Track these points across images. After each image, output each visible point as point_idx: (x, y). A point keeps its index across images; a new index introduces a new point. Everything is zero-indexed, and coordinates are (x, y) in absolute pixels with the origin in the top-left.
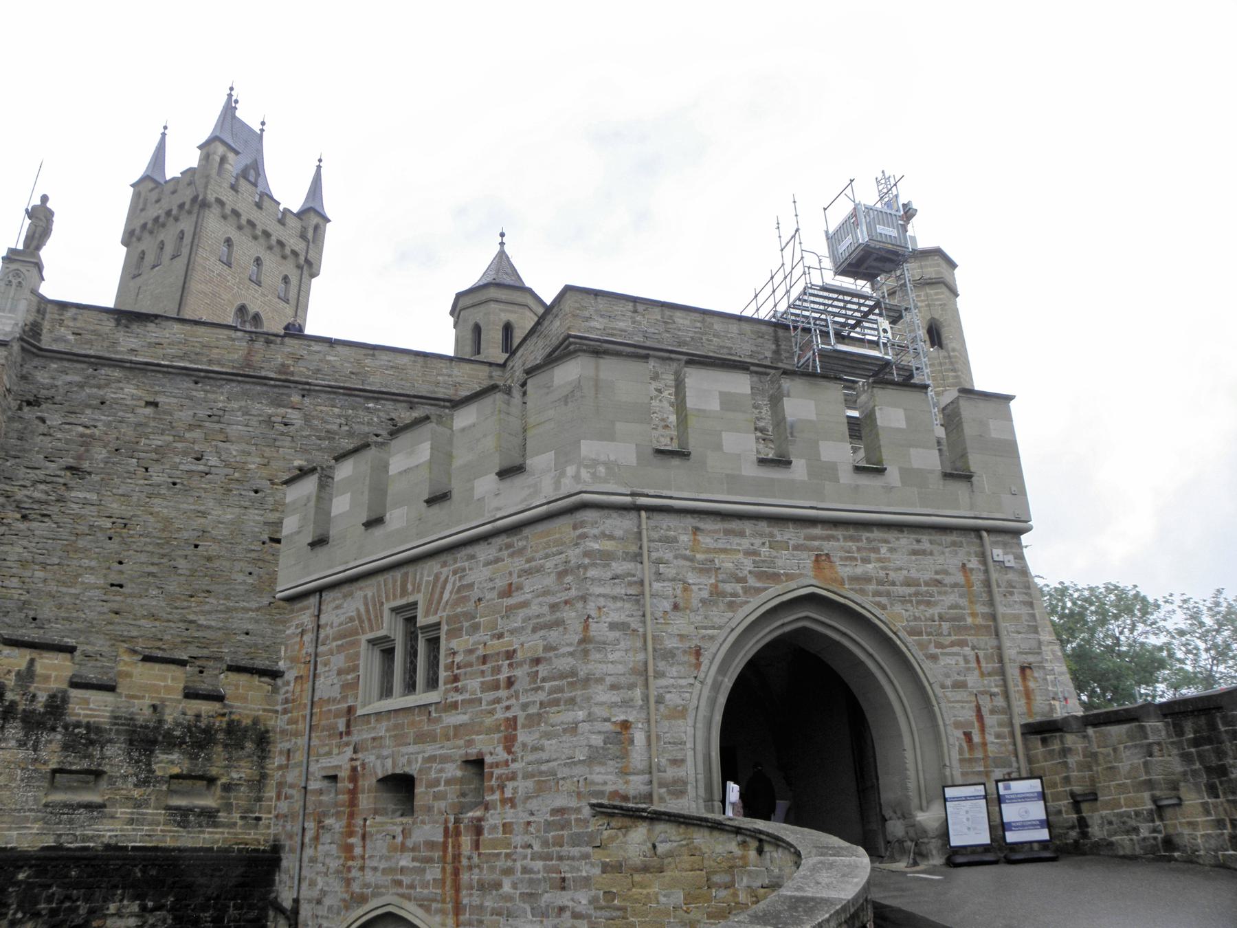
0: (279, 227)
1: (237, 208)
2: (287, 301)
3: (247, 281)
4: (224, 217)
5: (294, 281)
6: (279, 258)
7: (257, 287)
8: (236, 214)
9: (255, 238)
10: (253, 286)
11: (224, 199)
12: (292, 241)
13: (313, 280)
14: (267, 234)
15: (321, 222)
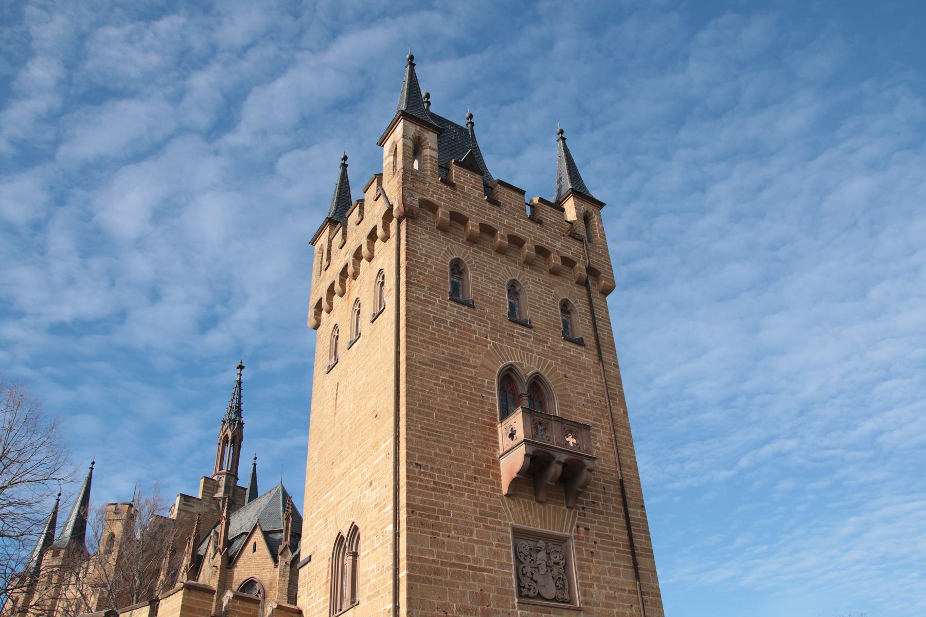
0: (532, 226)
1: (458, 210)
2: (580, 342)
3: (506, 324)
4: (443, 229)
5: (580, 306)
6: (545, 276)
7: (525, 331)
8: (458, 219)
9: (501, 251)
10: (518, 329)
11: (434, 199)
12: (558, 245)
13: (608, 298)
14: (516, 242)
15: (591, 208)
